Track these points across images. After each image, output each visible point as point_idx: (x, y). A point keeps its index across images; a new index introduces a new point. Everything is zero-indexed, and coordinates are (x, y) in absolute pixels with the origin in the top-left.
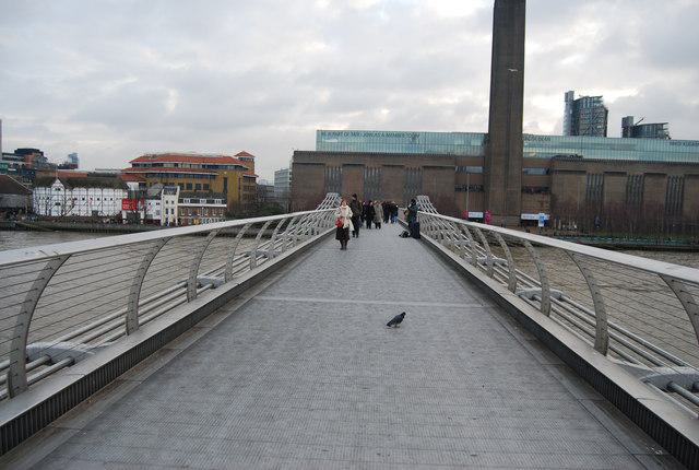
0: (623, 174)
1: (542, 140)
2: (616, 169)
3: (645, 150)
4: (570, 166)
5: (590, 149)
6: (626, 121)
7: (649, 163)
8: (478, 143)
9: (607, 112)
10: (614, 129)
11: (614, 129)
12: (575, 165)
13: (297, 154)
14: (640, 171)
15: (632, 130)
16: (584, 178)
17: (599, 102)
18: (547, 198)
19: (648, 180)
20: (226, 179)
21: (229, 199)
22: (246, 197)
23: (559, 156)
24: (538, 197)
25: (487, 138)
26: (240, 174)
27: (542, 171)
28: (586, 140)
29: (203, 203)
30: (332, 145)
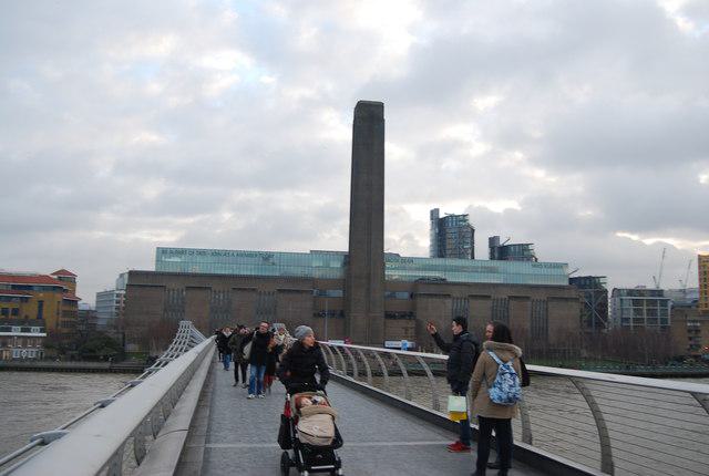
0: (488, 297)
1: (408, 262)
2: (480, 292)
3: (513, 272)
4: (433, 290)
5: (456, 272)
6: (493, 241)
7: (513, 286)
8: (337, 264)
9: (473, 231)
10: (482, 250)
11: (482, 250)
12: (439, 289)
13: (132, 274)
14: (504, 294)
15: (500, 251)
16: (449, 302)
17: (465, 221)
18: (412, 324)
19: (512, 303)
20: (41, 303)
21: (48, 325)
22: (65, 324)
23: (422, 279)
24: (403, 323)
25: (348, 259)
26: (59, 297)
27: (406, 295)
28: (450, 262)
29: (16, 332)
30: (174, 264)
